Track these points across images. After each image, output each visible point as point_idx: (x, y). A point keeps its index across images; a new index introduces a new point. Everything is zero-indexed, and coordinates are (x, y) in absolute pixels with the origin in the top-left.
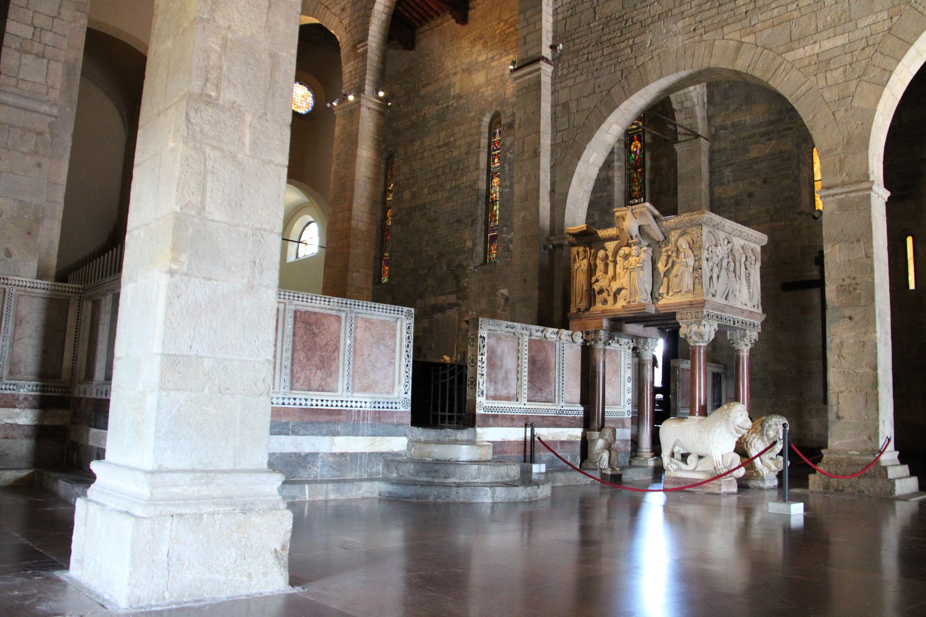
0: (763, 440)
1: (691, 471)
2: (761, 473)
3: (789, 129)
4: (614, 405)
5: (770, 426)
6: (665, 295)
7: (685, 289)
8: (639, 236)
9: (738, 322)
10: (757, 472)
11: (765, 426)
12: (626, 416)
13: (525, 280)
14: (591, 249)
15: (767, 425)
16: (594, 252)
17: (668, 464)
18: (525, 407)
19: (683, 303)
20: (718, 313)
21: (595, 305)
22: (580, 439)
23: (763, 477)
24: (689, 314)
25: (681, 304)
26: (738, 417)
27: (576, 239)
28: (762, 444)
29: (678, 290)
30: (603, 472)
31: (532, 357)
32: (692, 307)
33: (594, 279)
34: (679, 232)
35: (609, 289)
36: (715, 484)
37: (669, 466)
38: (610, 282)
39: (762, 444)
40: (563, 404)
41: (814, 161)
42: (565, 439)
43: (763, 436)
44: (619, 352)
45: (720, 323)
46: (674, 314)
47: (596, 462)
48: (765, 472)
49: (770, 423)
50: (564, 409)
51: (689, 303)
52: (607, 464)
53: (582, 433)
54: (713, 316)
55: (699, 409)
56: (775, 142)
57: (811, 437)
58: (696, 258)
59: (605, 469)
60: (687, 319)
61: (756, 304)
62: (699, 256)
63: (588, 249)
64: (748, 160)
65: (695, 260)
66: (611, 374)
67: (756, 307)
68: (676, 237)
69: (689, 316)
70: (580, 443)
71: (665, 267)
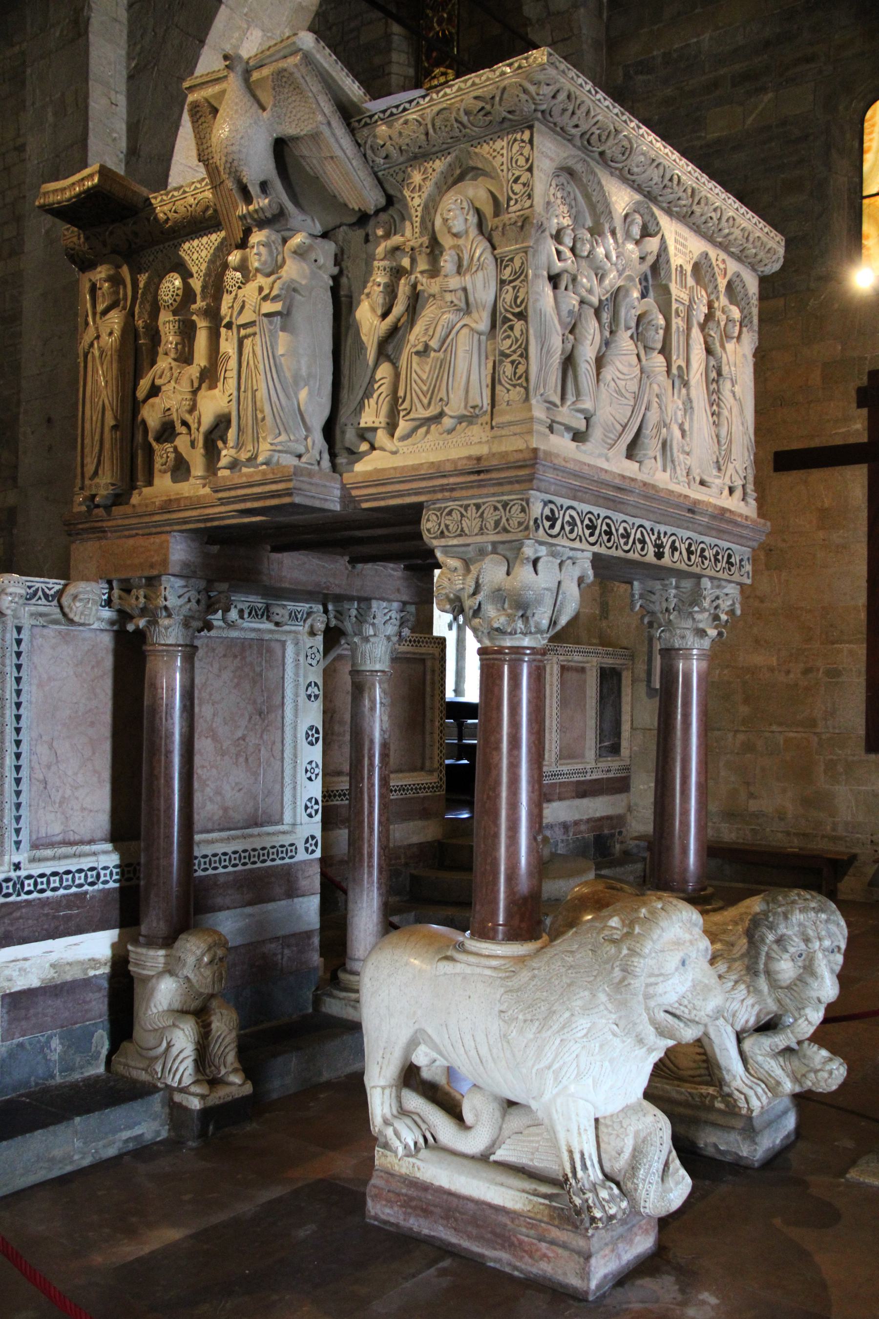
0: (753, 989)
1: (472, 1158)
2: (742, 1103)
3: (808, 60)
4: (257, 825)
5: (780, 941)
6: (381, 437)
7: (456, 407)
8: (278, 185)
9: (674, 548)
10: (727, 1097)
11: (763, 940)
12: (302, 856)
13: (49, 420)
14: (135, 271)
15: (771, 937)
16: (147, 285)
17: (386, 1122)
19: (449, 467)
20: (596, 510)
21: (150, 483)
22: (106, 970)
23: (750, 1118)
24: (472, 512)
25: (438, 471)
26: (666, 977)
27: (87, 238)
28: (750, 1001)
29: (427, 414)
30: (178, 1098)
32: (480, 484)
33: (144, 384)
34: (439, 165)
35: (189, 418)
36: (564, 1246)
37: (389, 1132)
38: (195, 392)
39: (750, 1001)
40: (20, 857)
41: (866, 145)
42: (35, 983)
43: (756, 974)
44: (277, 647)
45: (603, 550)
46: (414, 513)
47: (156, 1058)
48: (755, 1104)
49: (782, 930)
50: (23, 873)
51: (471, 465)
52: (190, 1070)
53: (114, 946)
54: (573, 524)
55: (509, 915)
56: (770, 95)
57: (834, 830)
58: (507, 274)
59: (183, 1090)
60: (462, 534)
61: (739, 483)
62: (517, 263)
63: (125, 271)
64: (701, 147)
65: (502, 282)
66: (243, 723)
67: (738, 493)
68: (429, 188)
69: (471, 523)
70: (106, 984)
71: (384, 316)
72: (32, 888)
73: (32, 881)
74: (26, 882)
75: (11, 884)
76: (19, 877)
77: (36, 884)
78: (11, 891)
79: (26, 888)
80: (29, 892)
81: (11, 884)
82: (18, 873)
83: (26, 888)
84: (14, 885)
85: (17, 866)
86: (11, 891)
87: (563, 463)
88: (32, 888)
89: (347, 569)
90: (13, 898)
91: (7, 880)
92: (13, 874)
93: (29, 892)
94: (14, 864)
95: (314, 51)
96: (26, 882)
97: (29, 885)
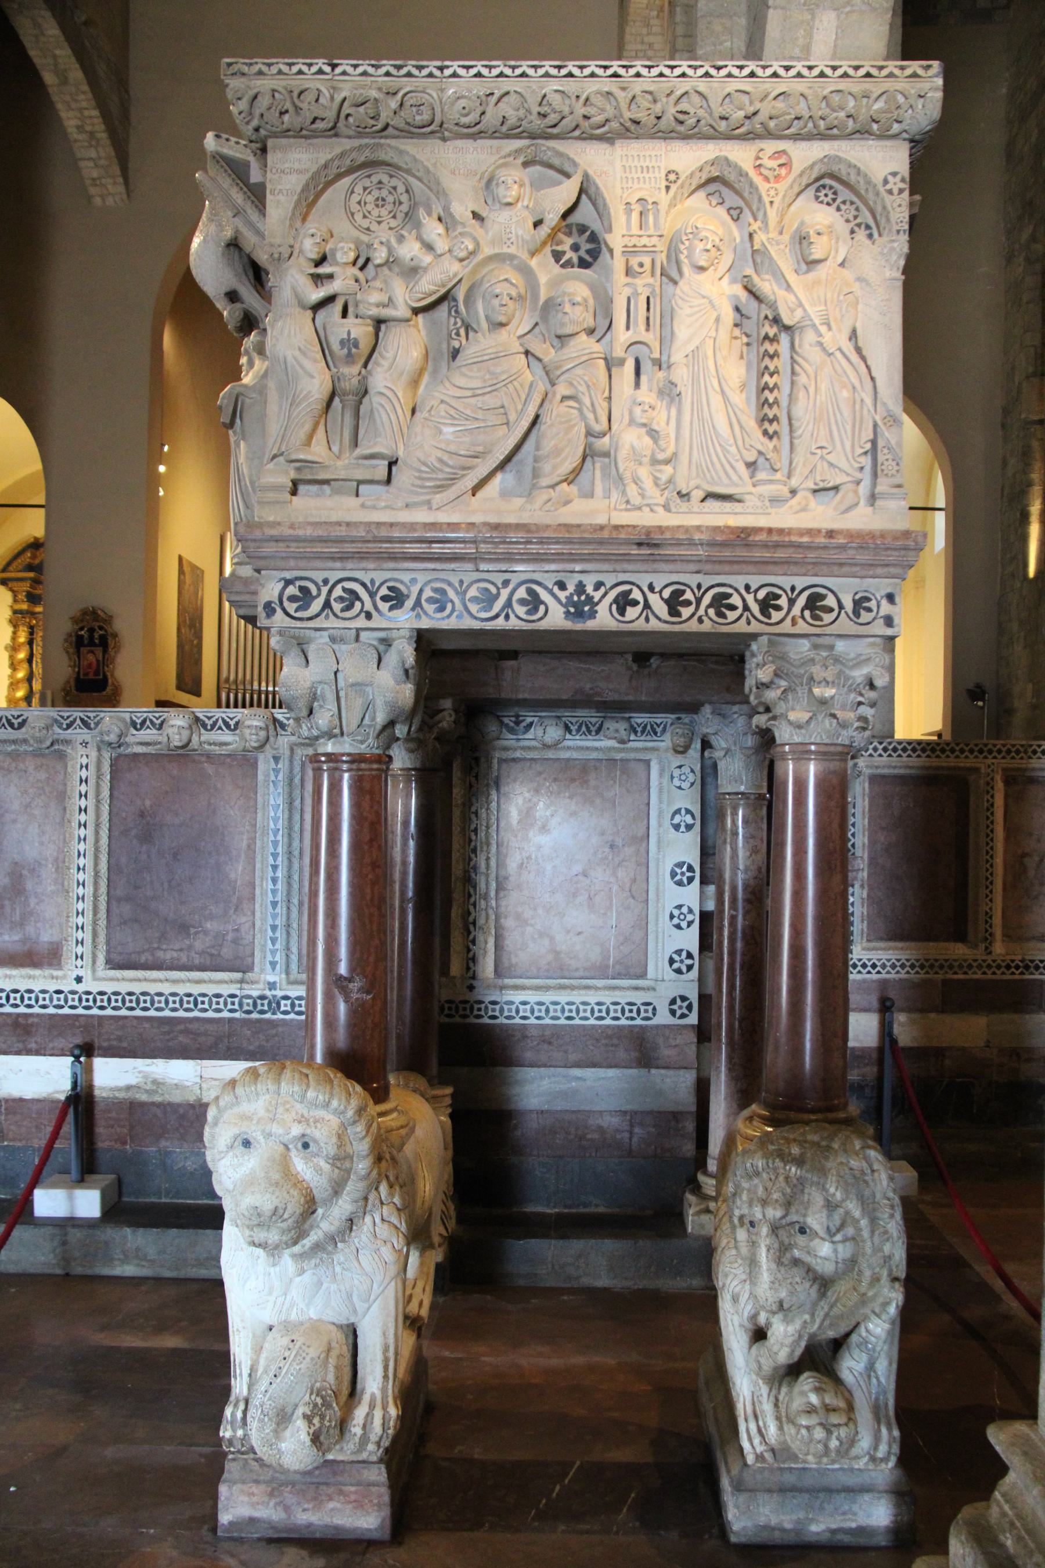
18: (81, 988)
31: (142, 815)
50: (279, 993)
72: (289, 1008)
73: (289, 1002)
74: (283, 1002)
75: (266, 1002)
76: (274, 996)
77: (293, 1005)
78: (266, 1008)
79: (283, 1008)
80: (286, 1013)
81: (266, 1002)
82: (274, 992)
83: (283, 1008)
84: (270, 1004)
85: (272, 986)
86: (266, 1008)
87: (291, 532)
88: (289, 1008)
89: (629, 668)
90: (268, 1016)
91: (263, 997)
92: (268, 993)
93: (286, 1013)
94: (269, 983)
95: (219, 149)
96: (283, 1002)
97: (285, 1005)
